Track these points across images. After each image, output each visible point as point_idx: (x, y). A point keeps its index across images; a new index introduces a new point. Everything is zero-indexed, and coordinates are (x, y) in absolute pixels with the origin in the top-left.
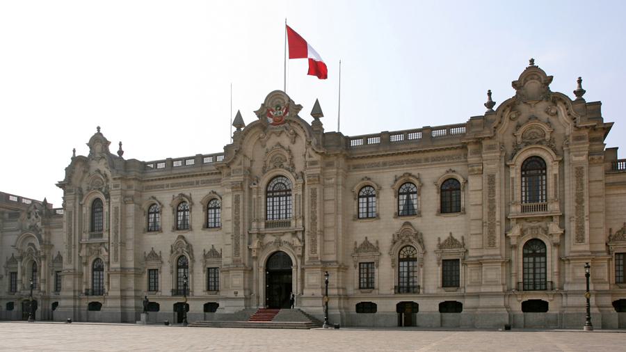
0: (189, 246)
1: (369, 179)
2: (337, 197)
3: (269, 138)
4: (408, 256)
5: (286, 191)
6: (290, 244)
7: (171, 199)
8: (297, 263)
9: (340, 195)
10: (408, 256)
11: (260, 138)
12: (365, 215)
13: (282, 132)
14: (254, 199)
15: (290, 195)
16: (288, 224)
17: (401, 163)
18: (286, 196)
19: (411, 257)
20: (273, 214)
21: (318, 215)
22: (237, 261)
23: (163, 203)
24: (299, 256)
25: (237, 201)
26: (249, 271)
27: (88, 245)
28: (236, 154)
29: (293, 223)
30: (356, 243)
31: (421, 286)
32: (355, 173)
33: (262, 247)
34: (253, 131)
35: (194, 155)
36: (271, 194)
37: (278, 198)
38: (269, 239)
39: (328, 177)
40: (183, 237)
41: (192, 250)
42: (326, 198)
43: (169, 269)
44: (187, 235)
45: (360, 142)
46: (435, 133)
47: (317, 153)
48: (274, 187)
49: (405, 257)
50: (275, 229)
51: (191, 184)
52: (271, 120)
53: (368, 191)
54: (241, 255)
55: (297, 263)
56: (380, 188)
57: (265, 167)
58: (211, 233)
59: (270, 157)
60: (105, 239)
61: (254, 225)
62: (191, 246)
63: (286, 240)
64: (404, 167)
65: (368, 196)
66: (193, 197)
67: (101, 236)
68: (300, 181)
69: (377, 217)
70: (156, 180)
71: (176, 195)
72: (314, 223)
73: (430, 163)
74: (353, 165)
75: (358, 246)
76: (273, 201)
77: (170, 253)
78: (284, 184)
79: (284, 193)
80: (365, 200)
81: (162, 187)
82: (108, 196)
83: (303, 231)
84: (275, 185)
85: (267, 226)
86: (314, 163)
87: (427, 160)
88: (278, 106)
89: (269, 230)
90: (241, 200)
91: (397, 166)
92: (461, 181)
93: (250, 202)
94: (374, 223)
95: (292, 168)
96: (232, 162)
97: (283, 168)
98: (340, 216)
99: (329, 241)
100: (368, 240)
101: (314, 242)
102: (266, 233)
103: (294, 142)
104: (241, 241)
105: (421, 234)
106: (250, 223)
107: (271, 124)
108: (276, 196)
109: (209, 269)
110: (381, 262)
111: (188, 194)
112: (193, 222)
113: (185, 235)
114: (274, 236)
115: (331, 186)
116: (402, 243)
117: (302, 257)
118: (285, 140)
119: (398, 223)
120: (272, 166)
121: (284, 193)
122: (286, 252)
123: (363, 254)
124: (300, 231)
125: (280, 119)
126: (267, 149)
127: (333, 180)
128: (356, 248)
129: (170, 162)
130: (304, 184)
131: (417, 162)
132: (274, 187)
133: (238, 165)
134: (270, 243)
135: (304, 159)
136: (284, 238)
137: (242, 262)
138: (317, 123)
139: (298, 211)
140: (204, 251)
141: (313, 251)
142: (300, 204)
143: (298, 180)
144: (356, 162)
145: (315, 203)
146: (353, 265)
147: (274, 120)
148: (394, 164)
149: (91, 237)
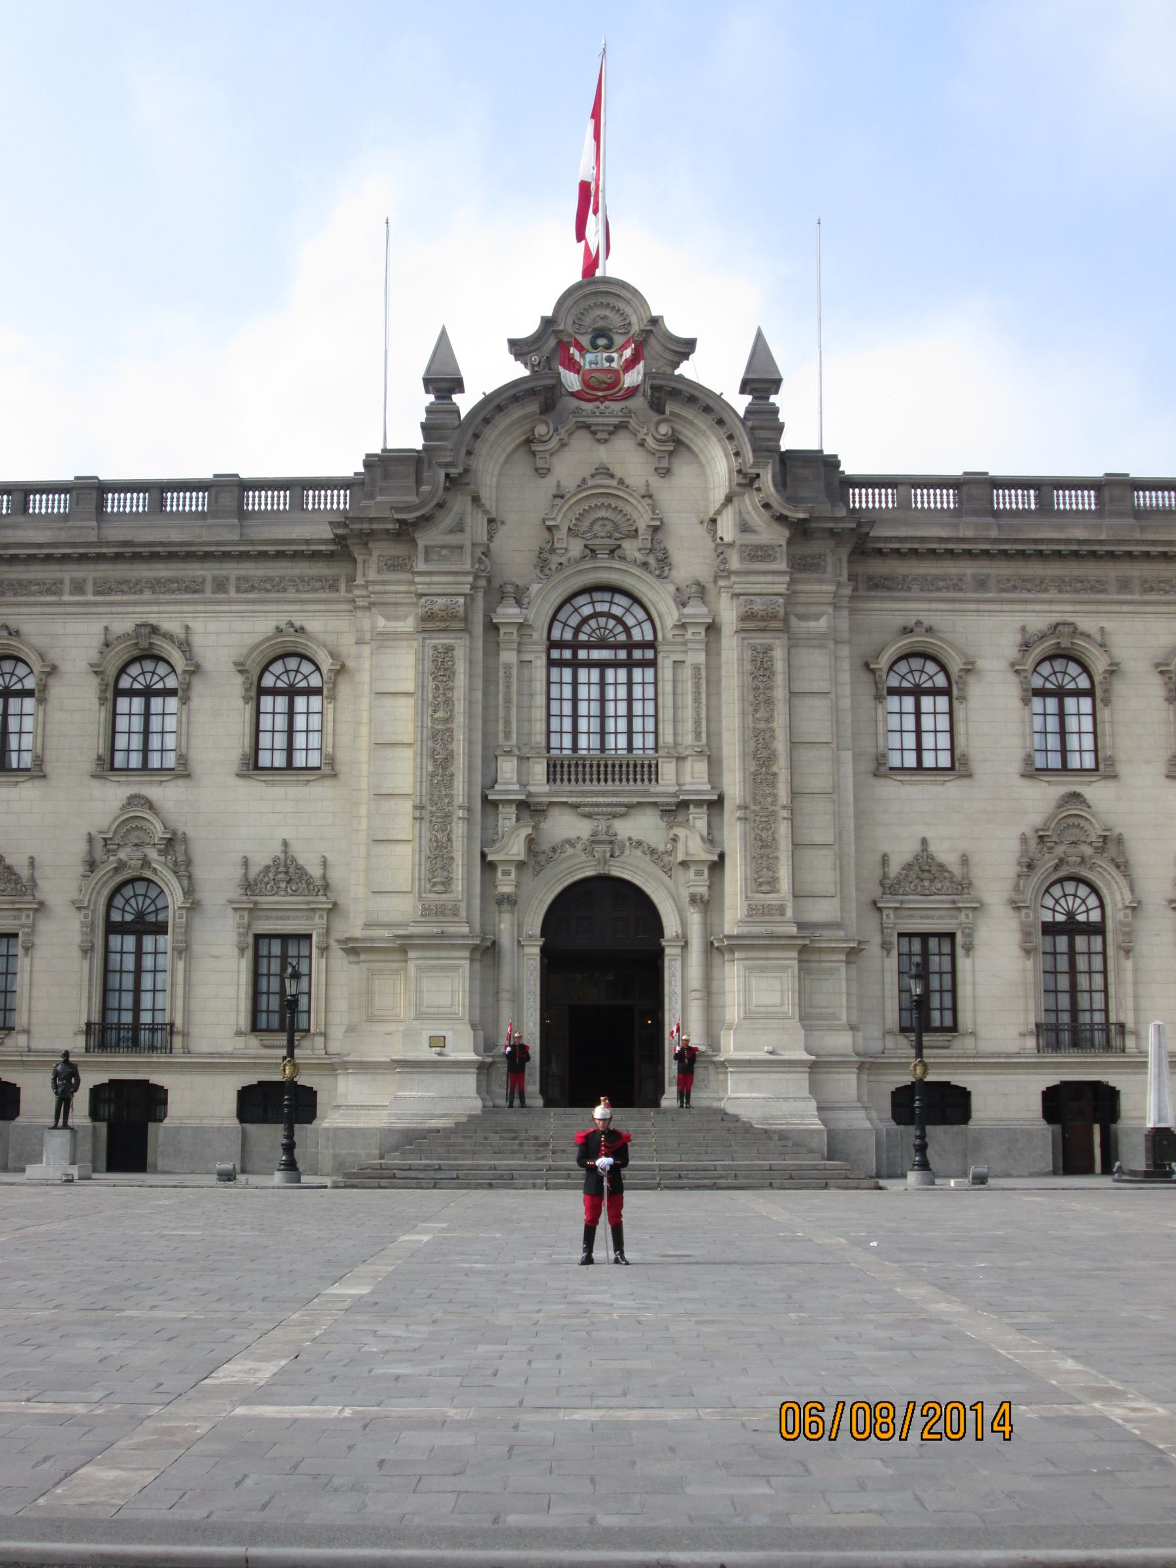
0: (172, 842)
1: (929, 630)
2: (835, 682)
3: (563, 445)
4: (1071, 915)
5: (630, 646)
6: (653, 852)
7: (97, 642)
8: (684, 924)
9: (845, 677)
10: (1071, 915)
11: (529, 441)
12: (910, 760)
13: (622, 427)
14: (508, 667)
15: (652, 663)
16: (650, 771)
17: (1041, 585)
18: (629, 664)
19: (1081, 918)
20: (575, 733)
21: (781, 746)
22: (440, 911)
23: (54, 655)
24: (693, 899)
25: (441, 669)
26: (487, 952)
28: (446, 489)
29: (667, 770)
30: (885, 860)
31: (1130, 1025)
32: (877, 605)
33: (536, 857)
34: (517, 413)
35: (205, 473)
36: (567, 654)
37: (595, 674)
38: (565, 826)
39: (801, 610)
40: (150, 805)
41: (189, 862)
42: (798, 686)
43: (77, 939)
44: (167, 795)
45: (884, 500)
46: (1145, 499)
47: (781, 519)
48: (577, 630)
49: (1060, 918)
50: (588, 787)
51: (194, 587)
52: (572, 380)
53: (925, 672)
54: (458, 887)
55: (684, 924)
56: (969, 669)
58: (278, 792)
59: (572, 516)
61: (507, 768)
62: (185, 839)
63: (636, 836)
64: (1051, 602)
65: (917, 692)
66: (198, 641)
68: (695, 610)
69: (958, 767)
70: (31, 559)
71: (123, 625)
73: (1136, 597)
74: (870, 578)
75: (894, 870)
76: (575, 684)
77: (81, 869)
78: (619, 620)
79: (622, 655)
80: (909, 703)
81: (54, 588)
83: (716, 805)
84: (585, 620)
85: (555, 770)
87: (1124, 585)
88: (601, 333)
89: (566, 791)
90: (461, 668)
91: (1026, 595)
93: (489, 680)
94: (953, 789)
95: (664, 561)
96: (426, 520)
97: (623, 558)
98: (847, 756)
99: (813, 845)
100: (933, 847)
101: (762, 852)
102: (551, 804)
103: (665, 473)
104: (459, 829)
105: (1120, 840)
106: (490, 758)
107: (573, 394)
108: (589, 664)
109: (258, 937)
110: (983, 934)
111: (172, 625)
112: (194, 742)
113: (153, 792)
114: (588, 816)
115: (818, 641)
116: (1056, 868)
117: (708, 904)
118: (629, 461)
119: (1039, 800)
120: (576, 548)
121: (622, 655)
122: (637, 881)
123: (914, 901)
124: (699, 803)
125: (608, 378)
126: (558, 486)
127: (822, 624)
128: (885, 876)
129: (91, 493)
130: (712, 628)
131: (1092, 589)
132: (577, 630)
133: (451, 531)
134: (569, 842)
135: (709, 540)
136: (625, 828)
137: (463, 913)
139: (689, 726)
140: (246, 863)
141: (762, 879)
142: (697, 700)
143: (686, 611)
144: (879, 568)
145: (769, 702)
146: (877, 940)
147: (585, 383)
148: (1015, 587)
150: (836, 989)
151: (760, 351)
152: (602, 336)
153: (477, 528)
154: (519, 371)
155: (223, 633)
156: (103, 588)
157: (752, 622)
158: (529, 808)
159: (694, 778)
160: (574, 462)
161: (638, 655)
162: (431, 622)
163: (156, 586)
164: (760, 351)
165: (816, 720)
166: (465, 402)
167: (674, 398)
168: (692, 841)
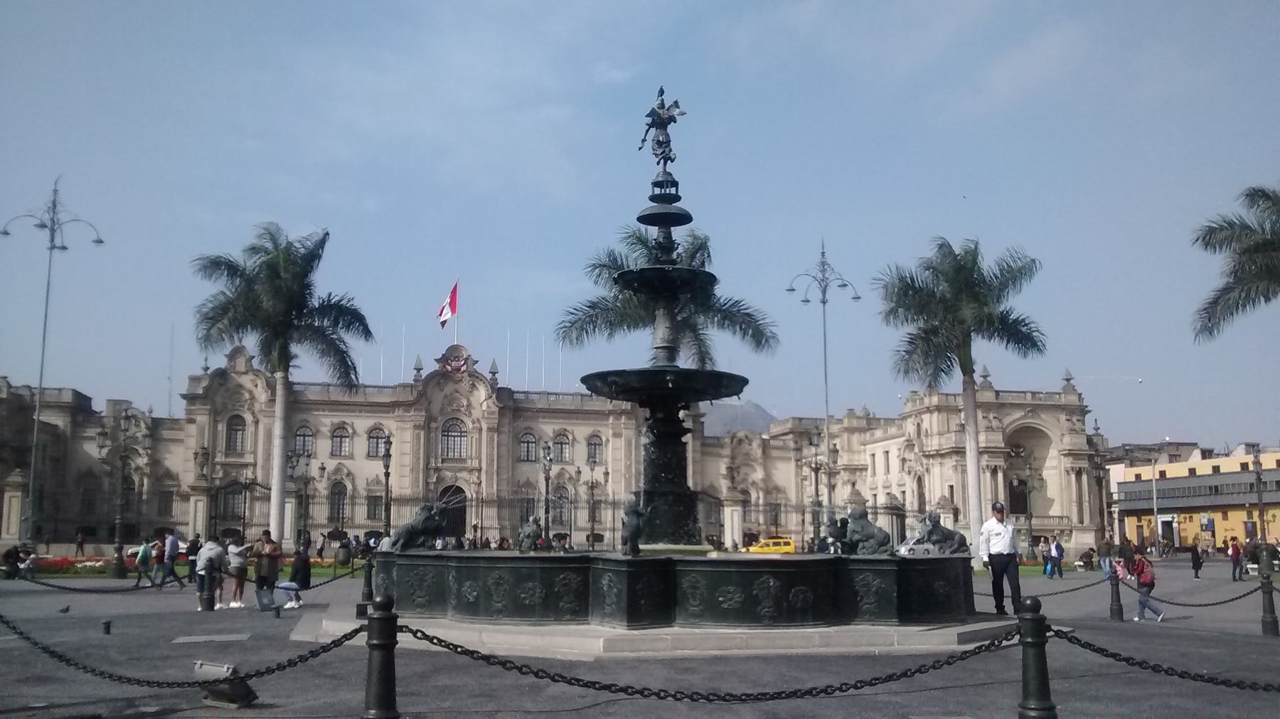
0: (349, 474)
11: (438, 383)
16: (464, 461)
27: (223, 465)
33: (440, 480)
57: (442, 410)
60: (249, 459)
61: (432, 460)
67: (242, 455)
68: (477, 425)
71: (336, 420)
72: (490, 464)
82: (253, 414)
83: (480, 470)
86: (493, 413)
92: (604, 439)
138: (494, 381)
149: (227, 456)
150: (506, 512)
151: (494, 364)
152: (457, 358)
153: (426, 404)
154: (436, 367)
155: (362, 423)
156: (330, 410)
157: (489, 429)
158: (437, 470)
159: (475, 464)
160: (449, 388)
161: (462, 434)
162: (416, 427)
163: (347, 411)
164: (494, 364)
165: (504, 451)
166: (424, 373)
167: (475, 376)
168: (474, 478)
